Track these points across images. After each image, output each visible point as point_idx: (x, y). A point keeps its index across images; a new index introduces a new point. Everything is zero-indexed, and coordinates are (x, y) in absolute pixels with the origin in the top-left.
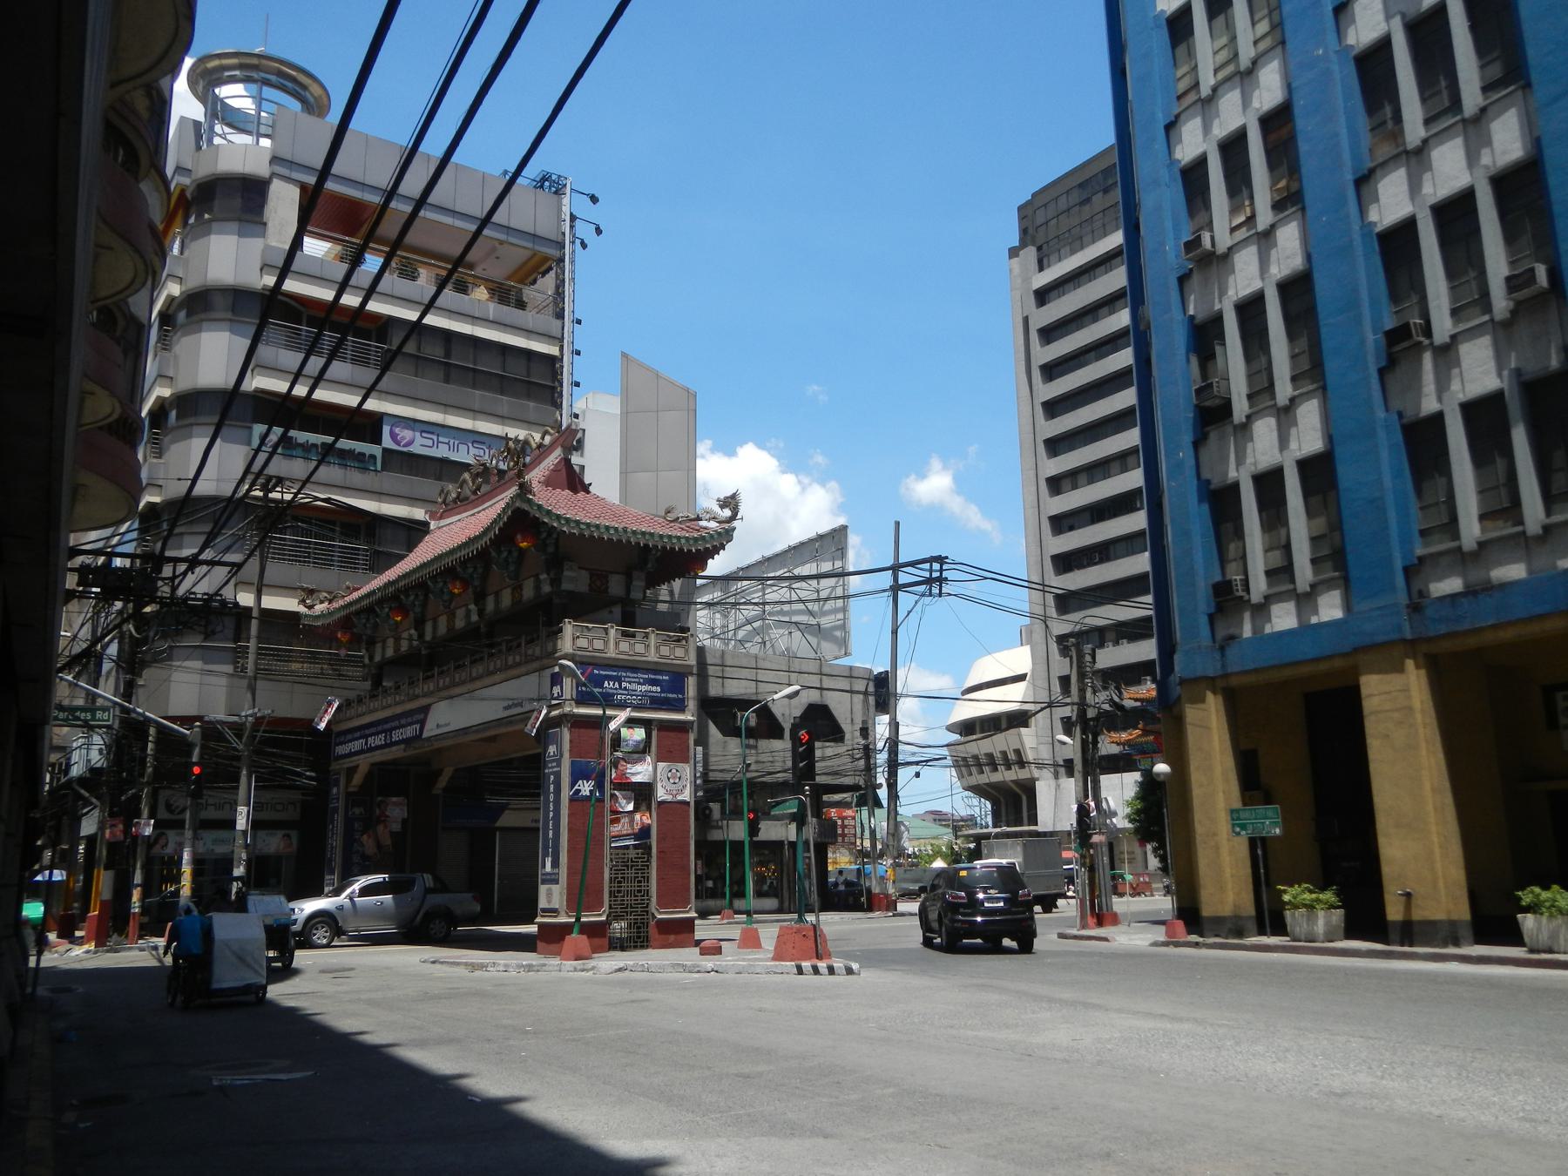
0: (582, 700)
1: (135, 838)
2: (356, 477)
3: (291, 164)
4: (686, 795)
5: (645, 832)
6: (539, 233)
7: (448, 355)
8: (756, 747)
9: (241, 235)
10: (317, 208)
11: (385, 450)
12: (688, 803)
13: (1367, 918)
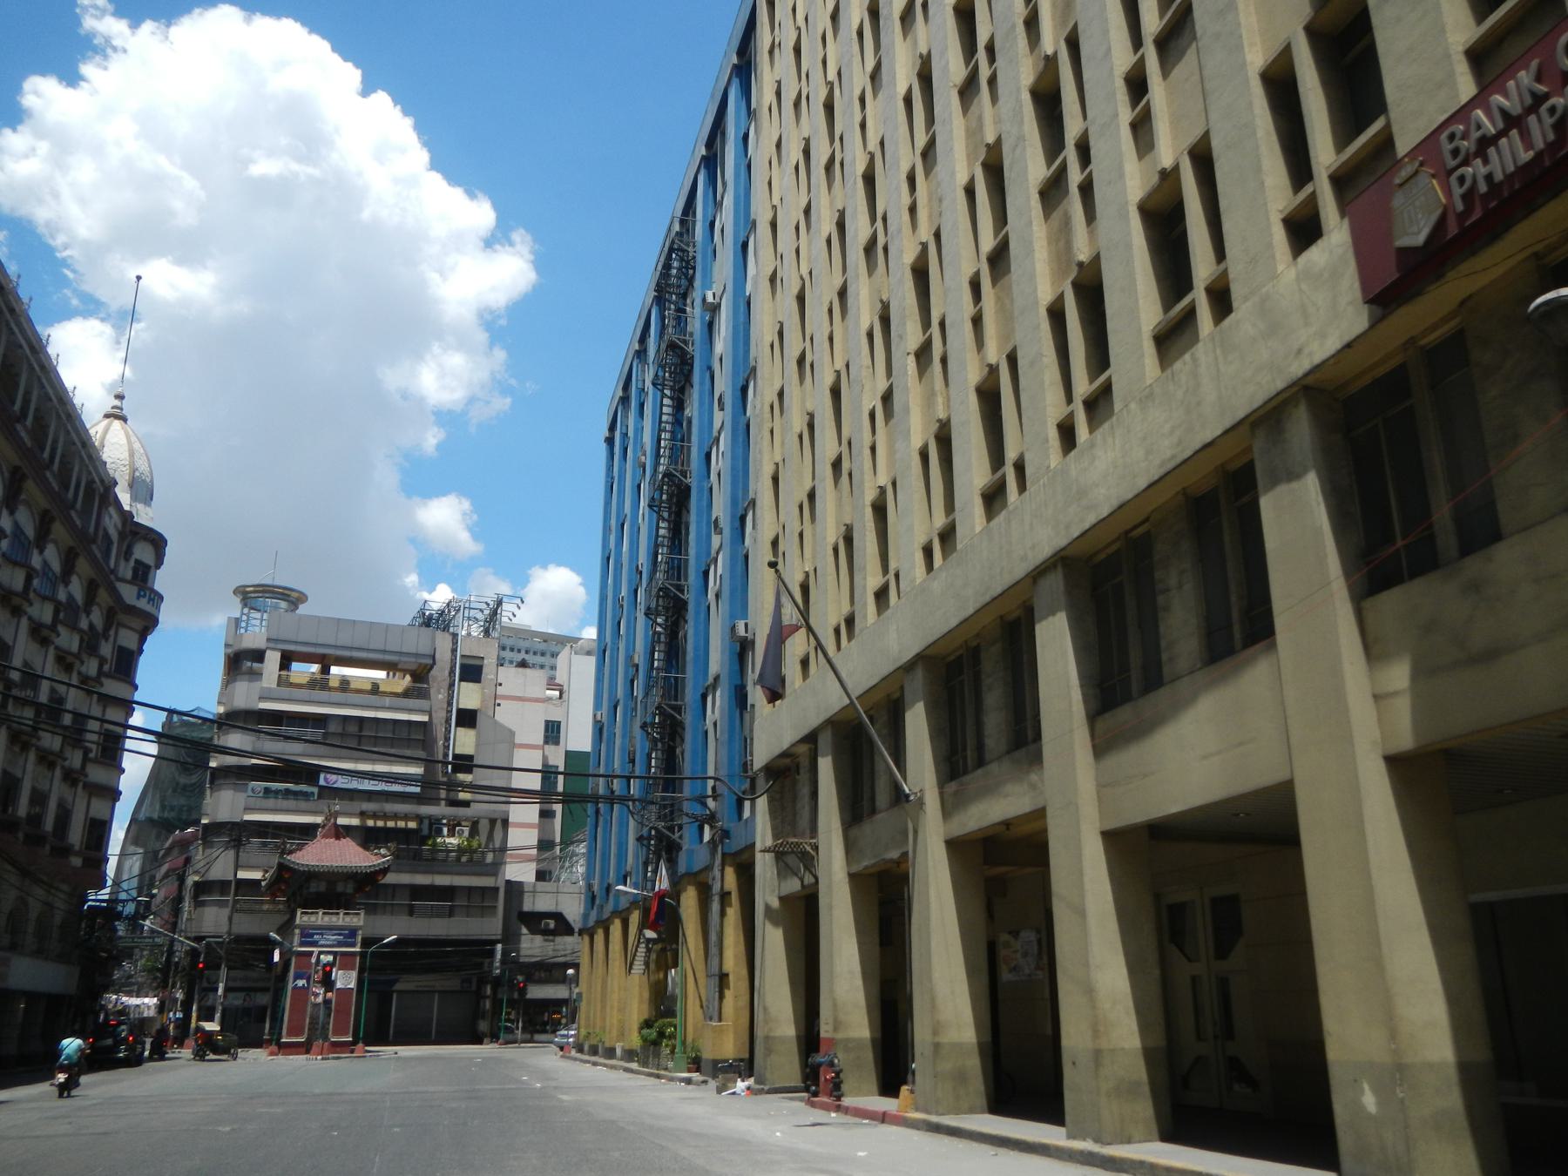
0: (302, 944)
2: (303, 804)
3: (276, 641)
4: (352, 986)
7: (361, 730)
10: (286, 661)
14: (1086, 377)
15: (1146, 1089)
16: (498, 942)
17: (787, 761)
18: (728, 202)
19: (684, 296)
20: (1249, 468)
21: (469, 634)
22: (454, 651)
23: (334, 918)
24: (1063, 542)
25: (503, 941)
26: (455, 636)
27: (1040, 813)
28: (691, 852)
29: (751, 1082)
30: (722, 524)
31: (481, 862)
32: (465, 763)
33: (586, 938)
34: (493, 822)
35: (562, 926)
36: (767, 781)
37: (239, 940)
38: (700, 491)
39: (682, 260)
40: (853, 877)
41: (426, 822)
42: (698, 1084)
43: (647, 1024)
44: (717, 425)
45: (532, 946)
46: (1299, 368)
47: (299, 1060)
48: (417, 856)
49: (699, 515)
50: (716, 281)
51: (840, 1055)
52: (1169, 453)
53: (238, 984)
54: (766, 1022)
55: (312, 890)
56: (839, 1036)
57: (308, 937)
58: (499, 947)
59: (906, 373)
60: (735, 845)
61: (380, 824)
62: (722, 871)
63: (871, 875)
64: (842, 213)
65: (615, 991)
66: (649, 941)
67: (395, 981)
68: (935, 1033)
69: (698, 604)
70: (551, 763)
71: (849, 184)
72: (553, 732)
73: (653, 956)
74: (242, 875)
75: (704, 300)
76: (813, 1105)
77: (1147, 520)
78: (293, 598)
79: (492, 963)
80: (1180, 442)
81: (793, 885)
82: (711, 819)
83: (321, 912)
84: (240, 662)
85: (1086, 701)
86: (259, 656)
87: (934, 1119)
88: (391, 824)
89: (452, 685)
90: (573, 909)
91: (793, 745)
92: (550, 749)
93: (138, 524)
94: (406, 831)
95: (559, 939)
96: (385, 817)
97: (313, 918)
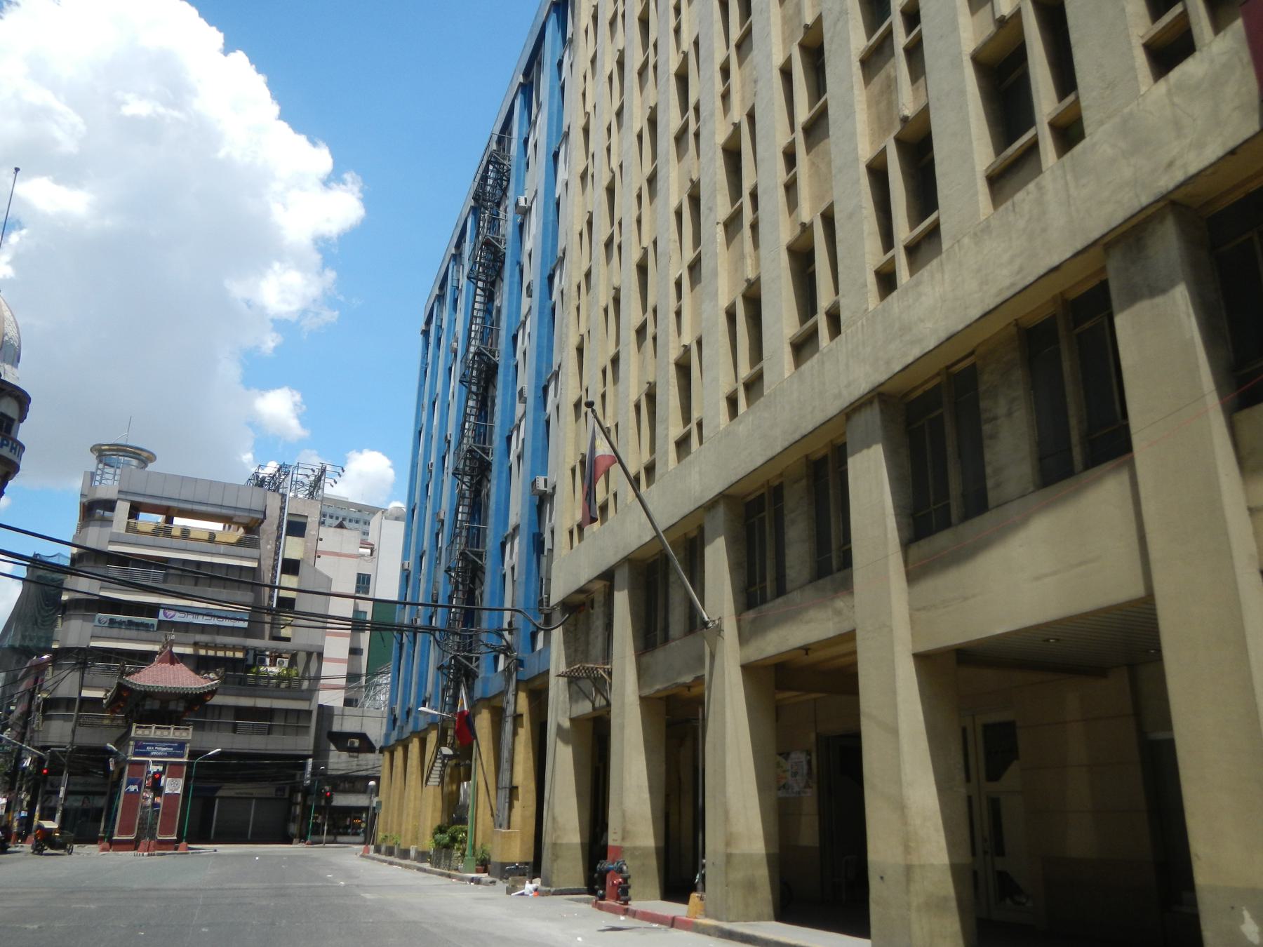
0: (136, 754)
2: (143, 634)
3: (126, 493)
6: (253, 507)
10: (135, 510)
14: (907, 225)
15: (953, 904)
16: (309, 757)
17: (582, 597)
18: (542, 120)
19: (498, 205)
20: (1104, 287)
21: (296, 496)
22: (282, 509)
23: (166, 733)
24: (882, 377)
26: (284, 496)
27: (849, 637)
28: (486, 680)
29: (537, 882)
30: (526, 394)
33: (387, 755)
34: (309, 654)
35: (365, 745)
36: (563, 615)
37: (81, 749)
38: (507, 367)
39: (498, 172)
40: (643, 699)
41: (251, 653)
42: (486, 884)
43: (441, 830)
44: (524, 310)
45: (338, 761)
46: (1167, 182)
47: (129, 855)
48: (242, 682)
49: (505, 387)
50: (529, 186)
51: (627, 862)
52: (1007, 282)
53: (78, 788)
54: (554, 829)
55: (147, 707)
56: (627, 844)
57: (141, 748)
58: (310, 761)
59: (714, 241)
60: (526, 673)
61: (211, 653)
62: (516, 696)
63: (660, 699)
64: (654, 110)
65: (411, 803)
66: (445, 756)
67: (217, 789)
68: (728, 844)
69: (501, 464)
71: (661, 82)
72: (363, 581)
73: (448, 770)
74: (86, 693)
75: (517, 204)
76: (600, 908)
77: (972, 353)
78: (143, 457)
80: (1020, 270)
81: (585, 708)
82: (508, 649)
83: (154, 726)
84: (94, 510)
85: (900, 529)
86: (110, 505)
87: (726, 926)
88: (220, 654)
89: (279, 537)
90: (376, 731)
91: (591, 581)
93: (4, 381)
94: (234, 660)
95: (362, 756)
96: (216, 647)
97: (147, 732)
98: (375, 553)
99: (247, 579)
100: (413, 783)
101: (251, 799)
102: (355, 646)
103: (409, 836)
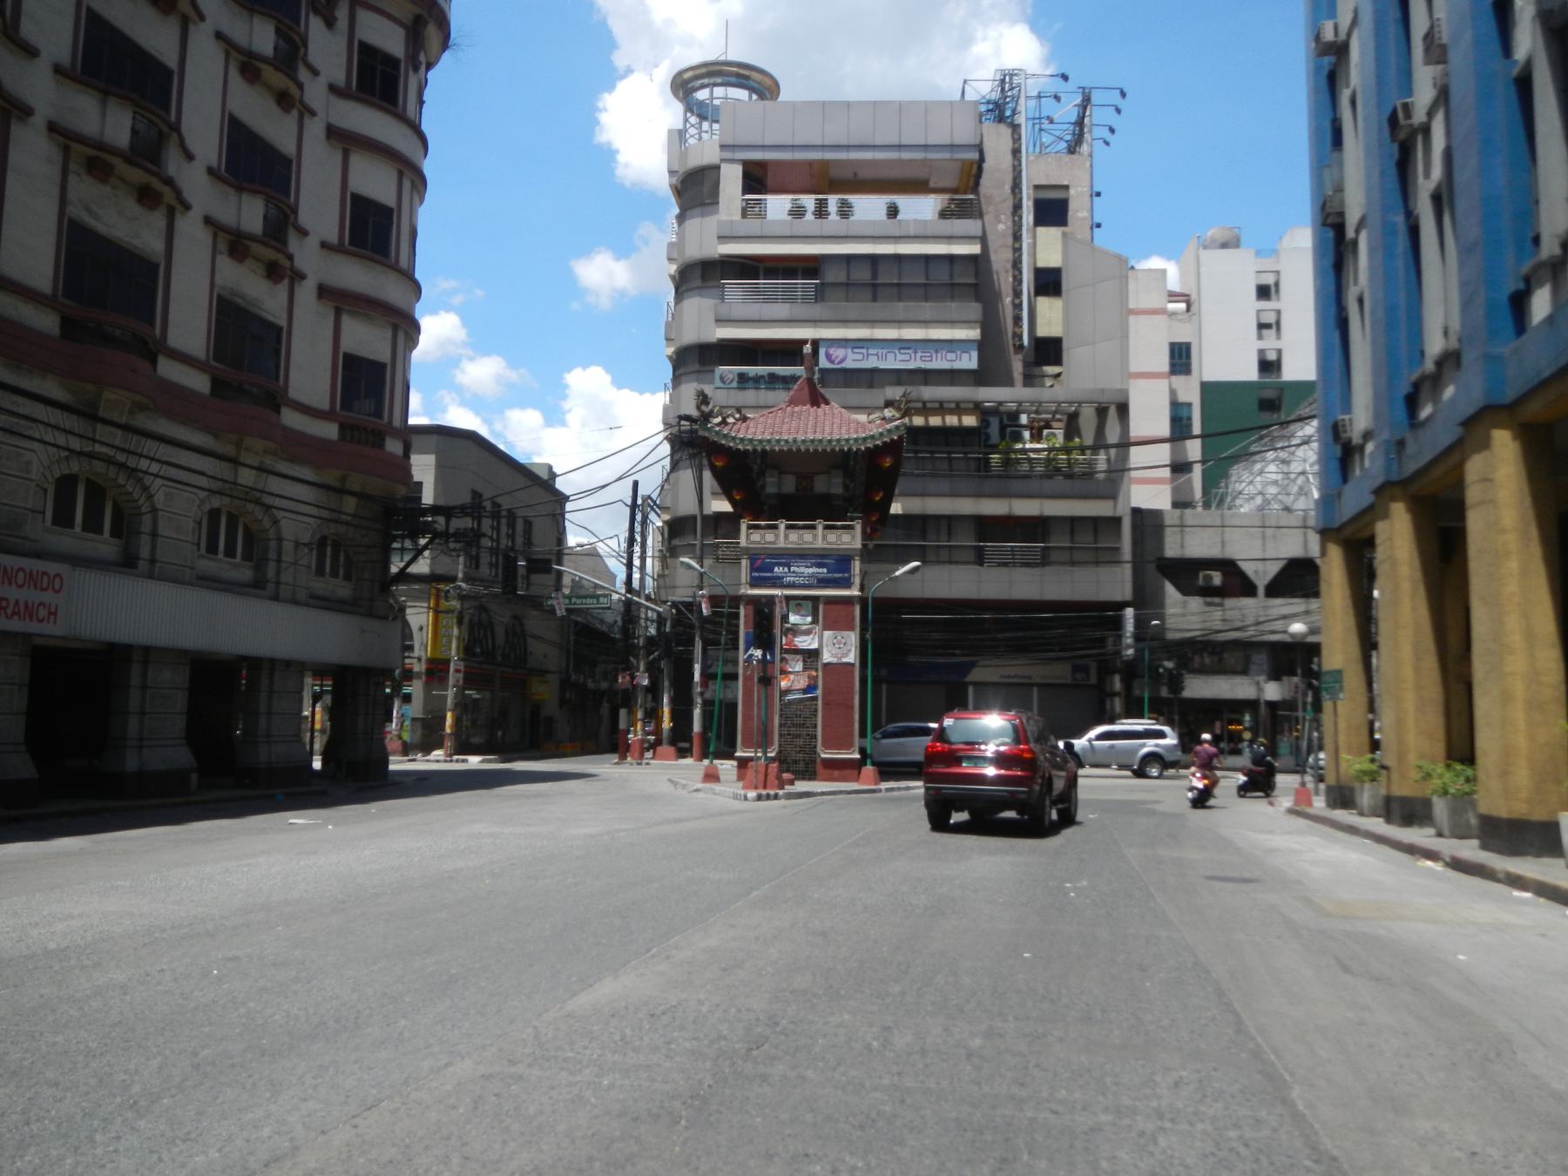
0: (754, 583)
1: (635, 687)
5: (810, 688)
6: (957, 141)
7: (875, 275)
8: (1221, 605)
9: (703, 215)
10: (757, 179)
11: (823, 371)
12: (852, 665)
13: (1473, 792)
16: (1126, 604)
23: (807, 536)
25: (1136, 603)
26: (1015, 128)
31: (1089, 475)
32: (1048, 351)
35: (1235, 581)
45: (1184, 614)
55: (771, 490)
58: (1129, 612)
70: (1182, 398)
72: (1181, 358)
79: (1120, 637)
88: (935, 421)
92: (1179, 381)
95: (1230, 602)
97: (770, 536)
98: (1193, 308)
99: (966, 281)
100: (1512, 587)
101: (1032, 685)
102: (1181, 459)
103: (1522, 776)
